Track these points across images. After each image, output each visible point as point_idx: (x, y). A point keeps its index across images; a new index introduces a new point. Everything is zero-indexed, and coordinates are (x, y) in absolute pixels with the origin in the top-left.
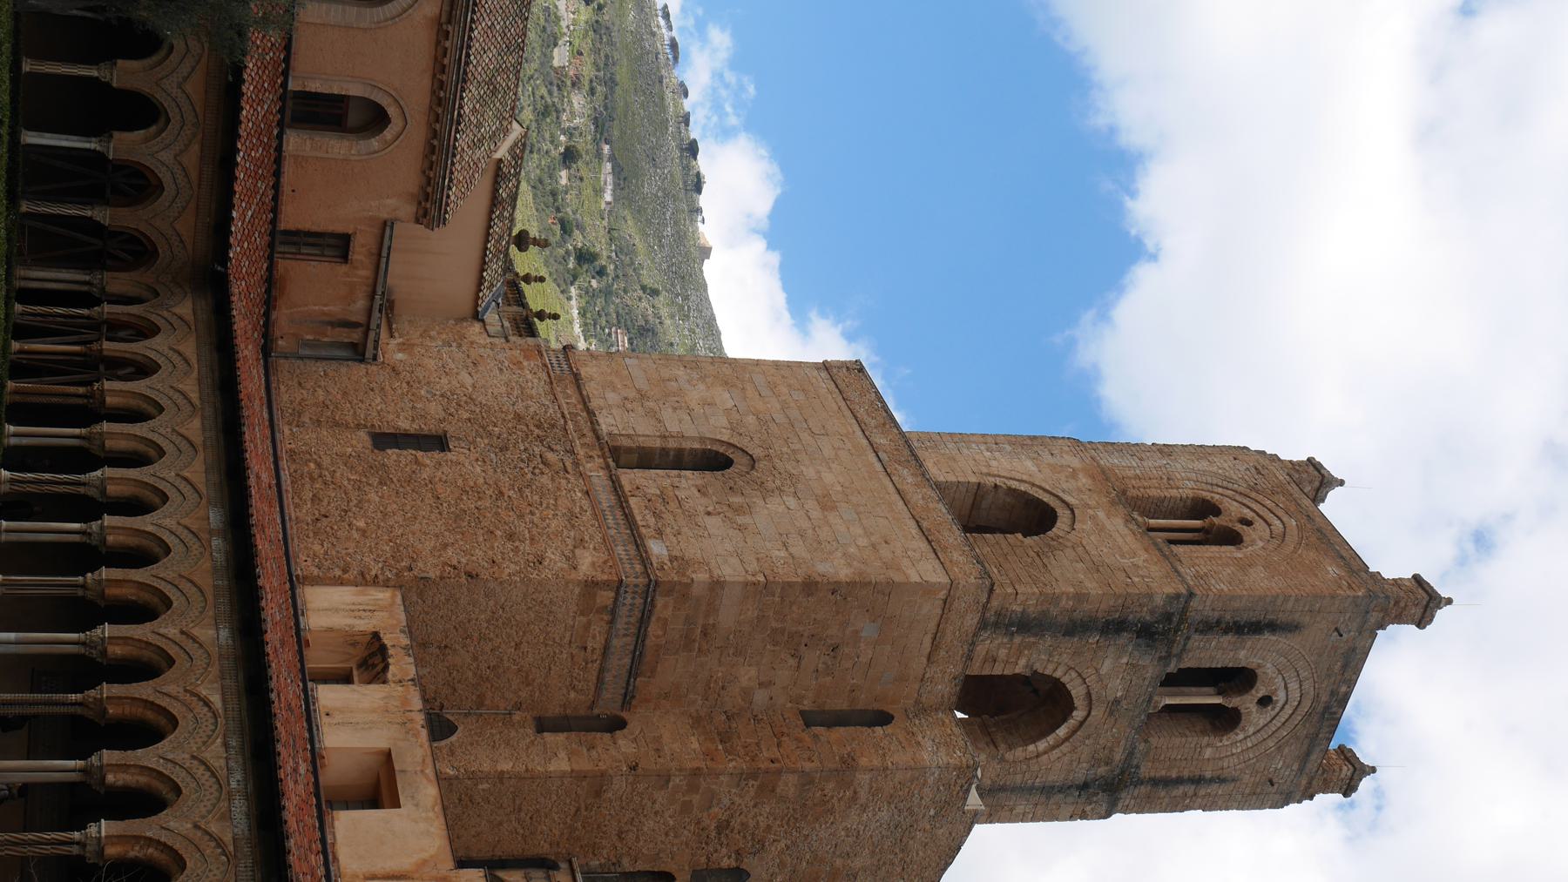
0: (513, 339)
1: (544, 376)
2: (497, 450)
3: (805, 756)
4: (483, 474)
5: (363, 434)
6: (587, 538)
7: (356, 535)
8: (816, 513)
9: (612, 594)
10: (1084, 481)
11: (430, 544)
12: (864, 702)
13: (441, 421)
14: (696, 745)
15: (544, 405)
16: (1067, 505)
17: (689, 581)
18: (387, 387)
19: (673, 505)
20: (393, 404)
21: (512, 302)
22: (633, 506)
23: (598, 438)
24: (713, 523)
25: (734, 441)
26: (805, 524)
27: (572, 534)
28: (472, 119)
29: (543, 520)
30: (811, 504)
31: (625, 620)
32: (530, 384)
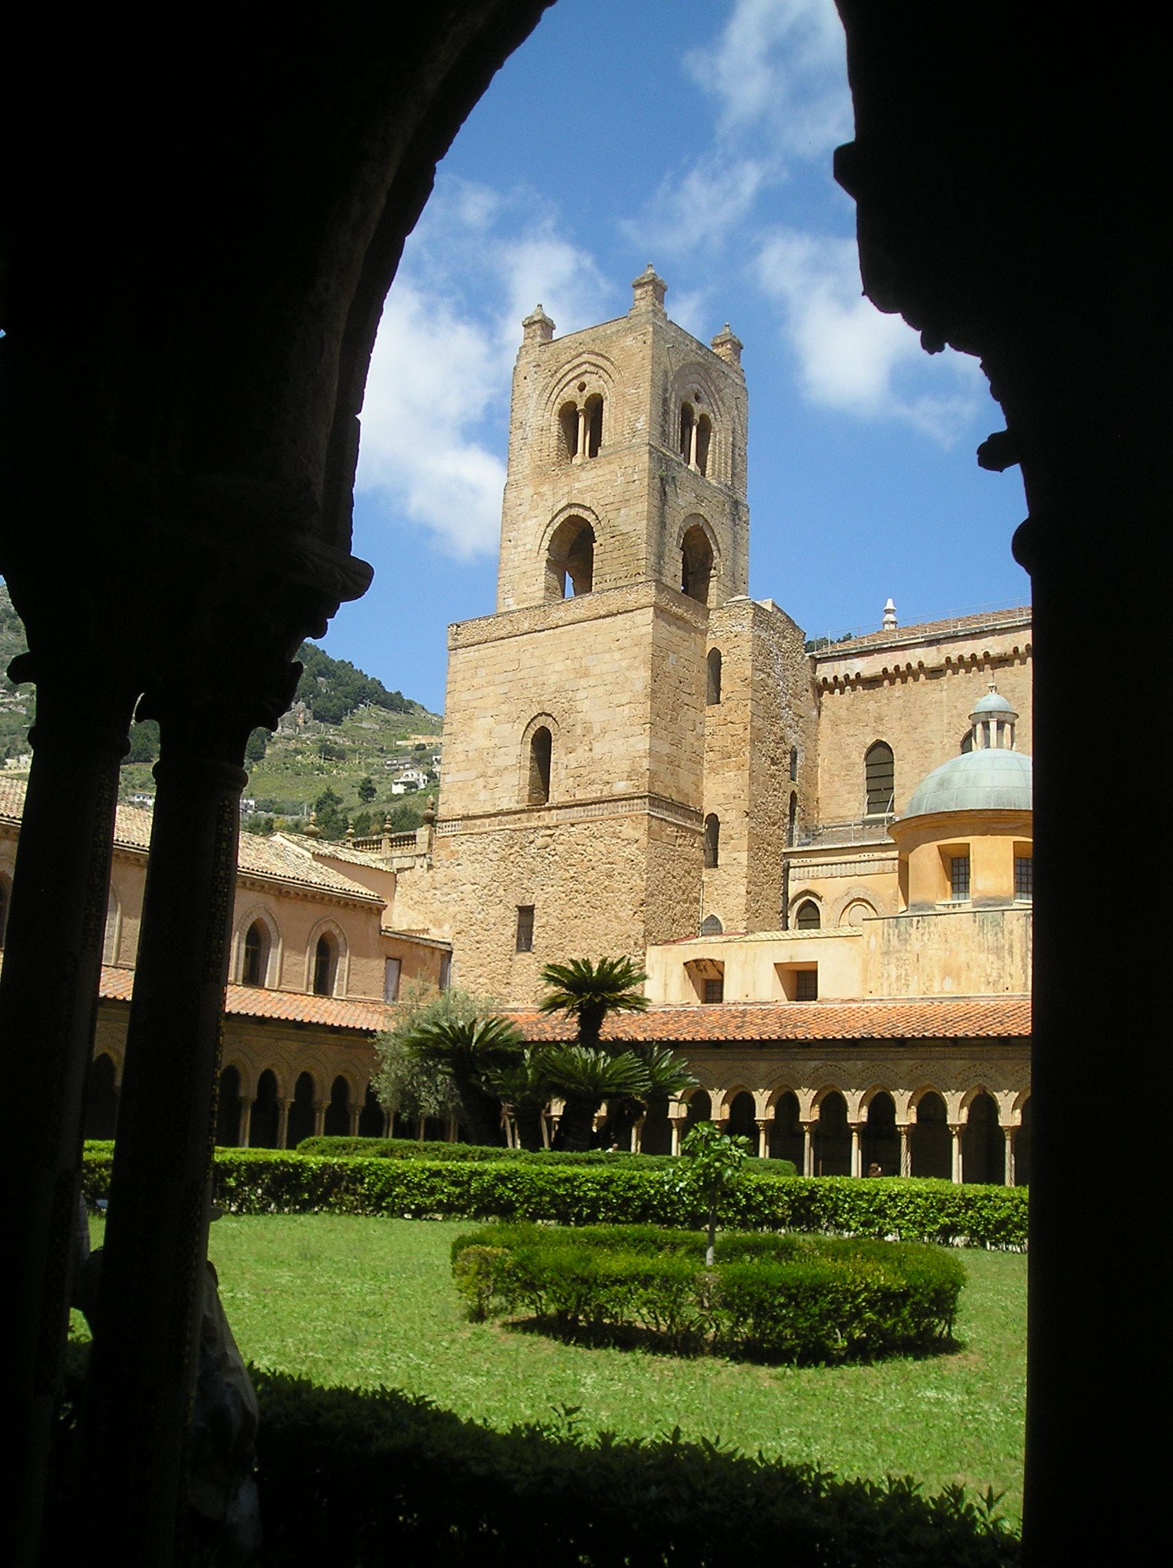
1: (463, 839)
3: (743, 708)
5: (516, 958)
10: (545, 489)
14: (732, 773)
16: (570, 506)
19: (582, 771)
22: (583, 797)
23: (522, 811)
25: (526, 725)
26: (600, 690)
29: (595, 855)
30: (583, 682)
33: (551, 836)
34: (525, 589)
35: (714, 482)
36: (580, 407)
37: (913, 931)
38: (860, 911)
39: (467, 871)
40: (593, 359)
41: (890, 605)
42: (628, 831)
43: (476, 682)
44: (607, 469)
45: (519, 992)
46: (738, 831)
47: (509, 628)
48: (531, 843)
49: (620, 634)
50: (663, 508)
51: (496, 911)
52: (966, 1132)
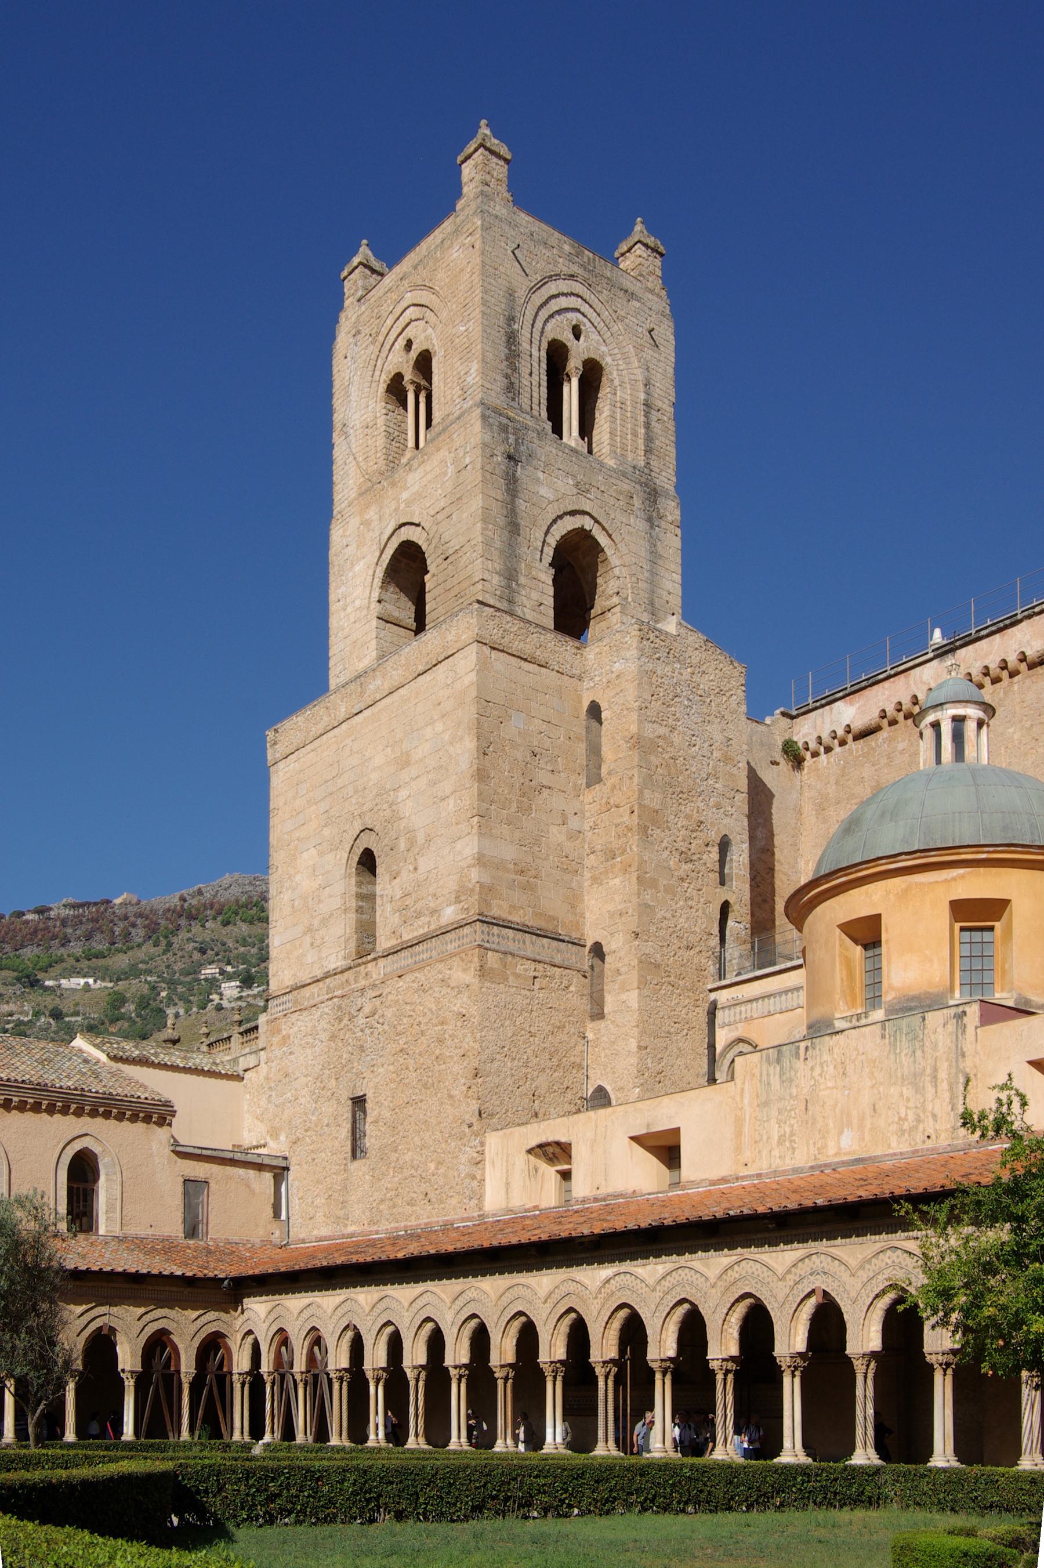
0: (261, 1043)
2: (363, 1055)
4: (385, 1066)
6: (440, 976)
9: (490, 953)
13: (339, 1102)
15: (321, 1016)
17: (478, 885)
18: (311, 1147)
20: (326, 1143)
21: (228, 1046)
22: (410, 937)
24: (425, 864)
27: (437, 989)
28: (75, 1079)
31: (511, 943)
32: (302, 1028)
35: (611, 463)
37: (799, 1064)
50: (513, 502)
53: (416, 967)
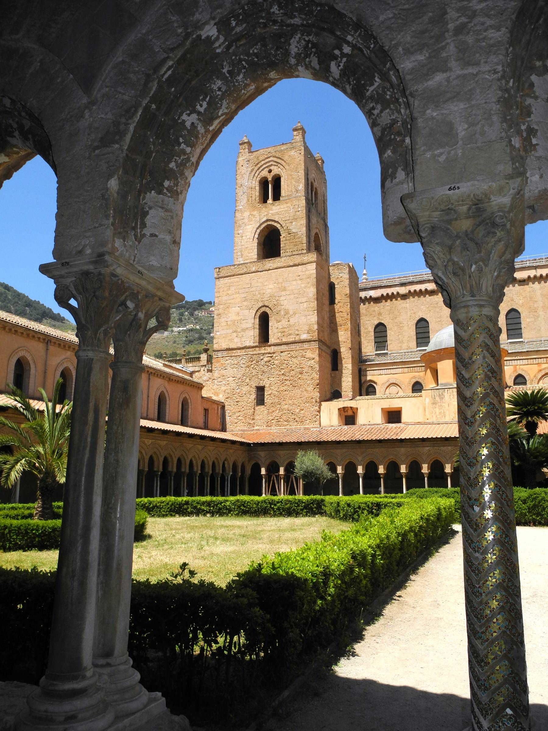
1: (227, 358)
5: (257, 408)
7: (302, 412)
8: (288, 293)
10: (255, 213)
11: (305, 393)
12: (327, 288)
14: (343, 333)
19: (285, 330)
22: (286, 340)
23: (256, 347)
24: (292, 321)
26: (292, 296)
29: (293, 364)
30: (283, 293)
33: (271, 357)
34: (248, 255)
36: (270, 179)
38: (393, 389)
39: (230, 372)
40: (275, 159)
41: (365, 272)
42: (309, 354)
43: (229, 292)
44: (285, 206)
45: (259, 423)
46: (347, 355)
47: (245, 270)
48: (262, 360)
49: (300, 273)
51: (245, 389)
52: (386, 476)
53: (289, 350)
